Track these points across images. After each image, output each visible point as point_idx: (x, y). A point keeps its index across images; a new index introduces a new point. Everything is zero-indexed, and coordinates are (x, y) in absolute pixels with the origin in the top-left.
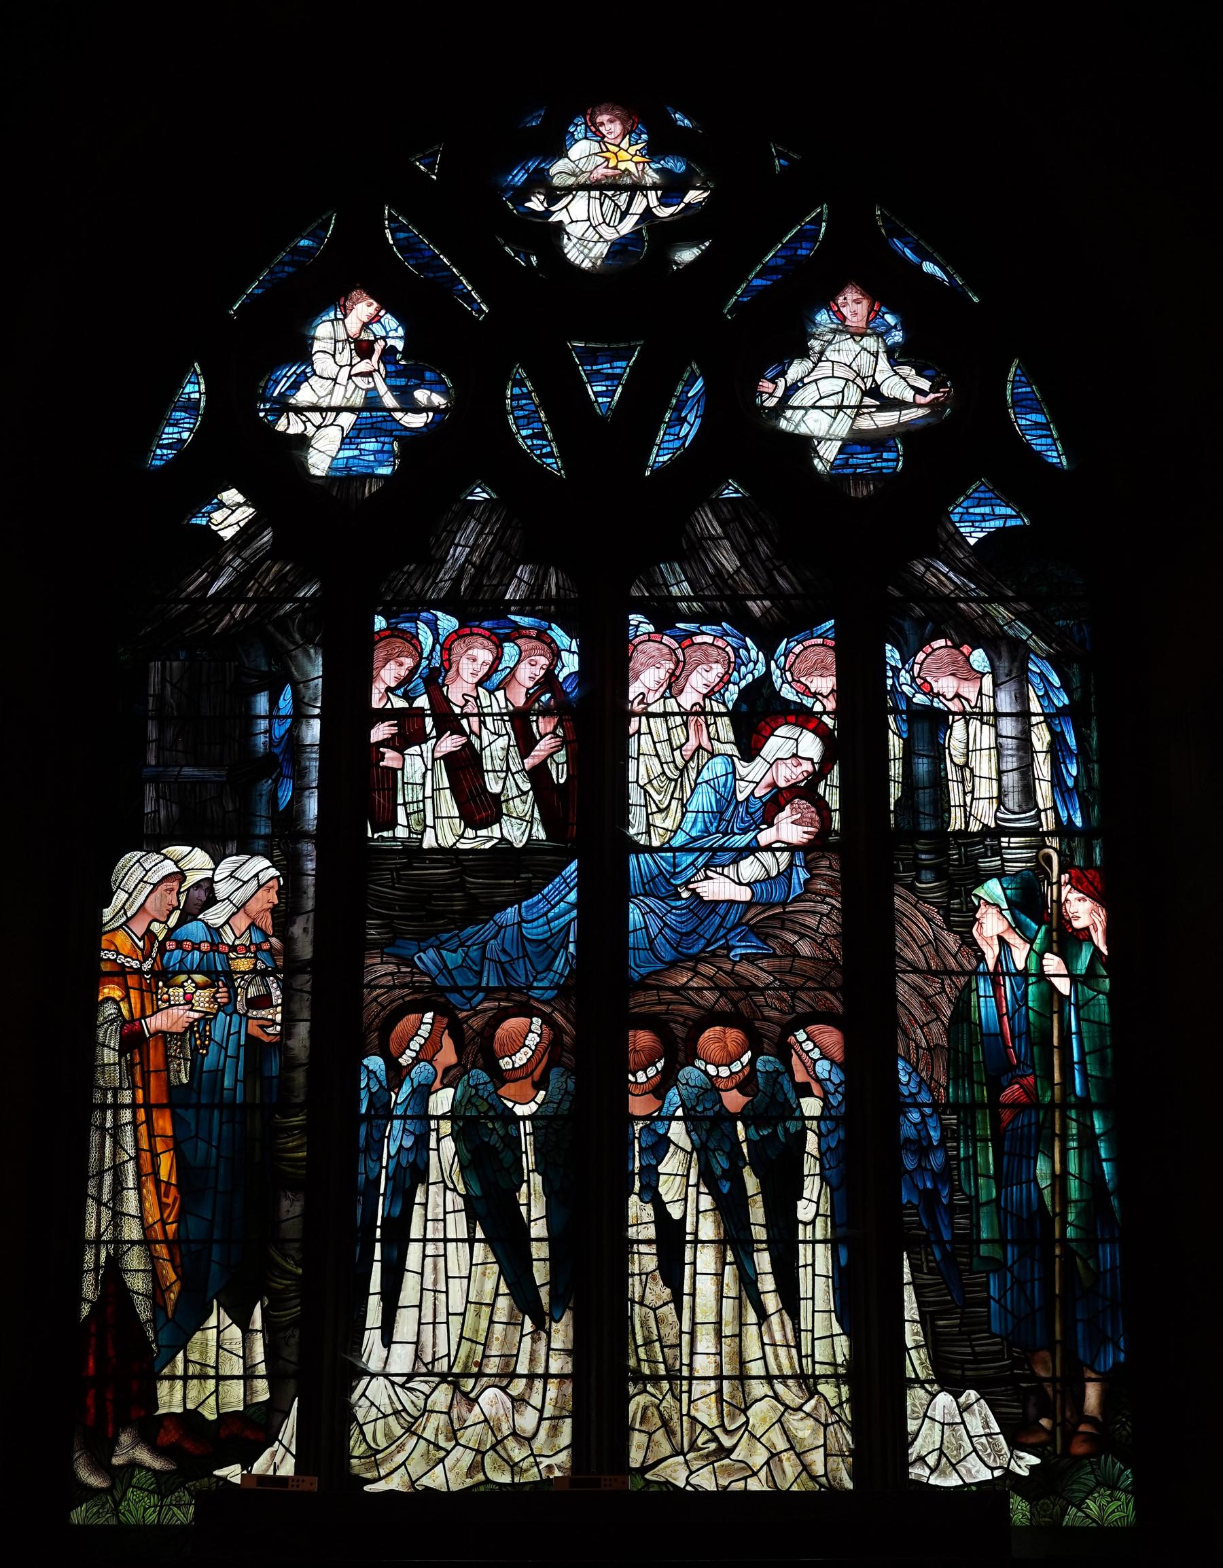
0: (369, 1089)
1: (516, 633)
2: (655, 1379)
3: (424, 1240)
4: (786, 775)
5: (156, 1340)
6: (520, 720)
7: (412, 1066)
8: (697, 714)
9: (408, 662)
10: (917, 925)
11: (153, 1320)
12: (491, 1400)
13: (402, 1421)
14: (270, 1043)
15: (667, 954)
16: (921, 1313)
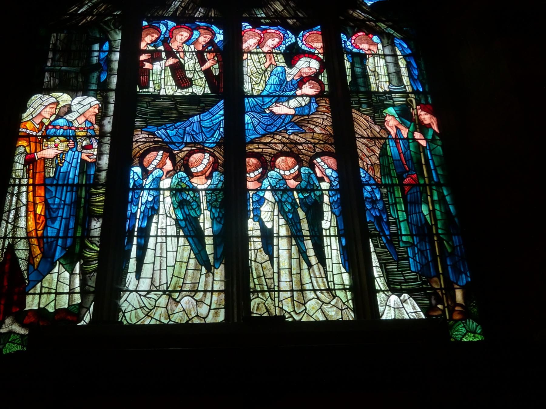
0: (134, 179)
1: (198, 28)
2: (263, 291)
3: (156, 236)
4: (306, 72)
5: (28, 278)
7: (153, 170)
8: (270, 53)
9: (156, 36)
10: (362, 124)
11: (28, 270)
12: (186, 301)
13: (144, 311)
14: (91, 162)
15: (262, 132)
16: (380, 264)
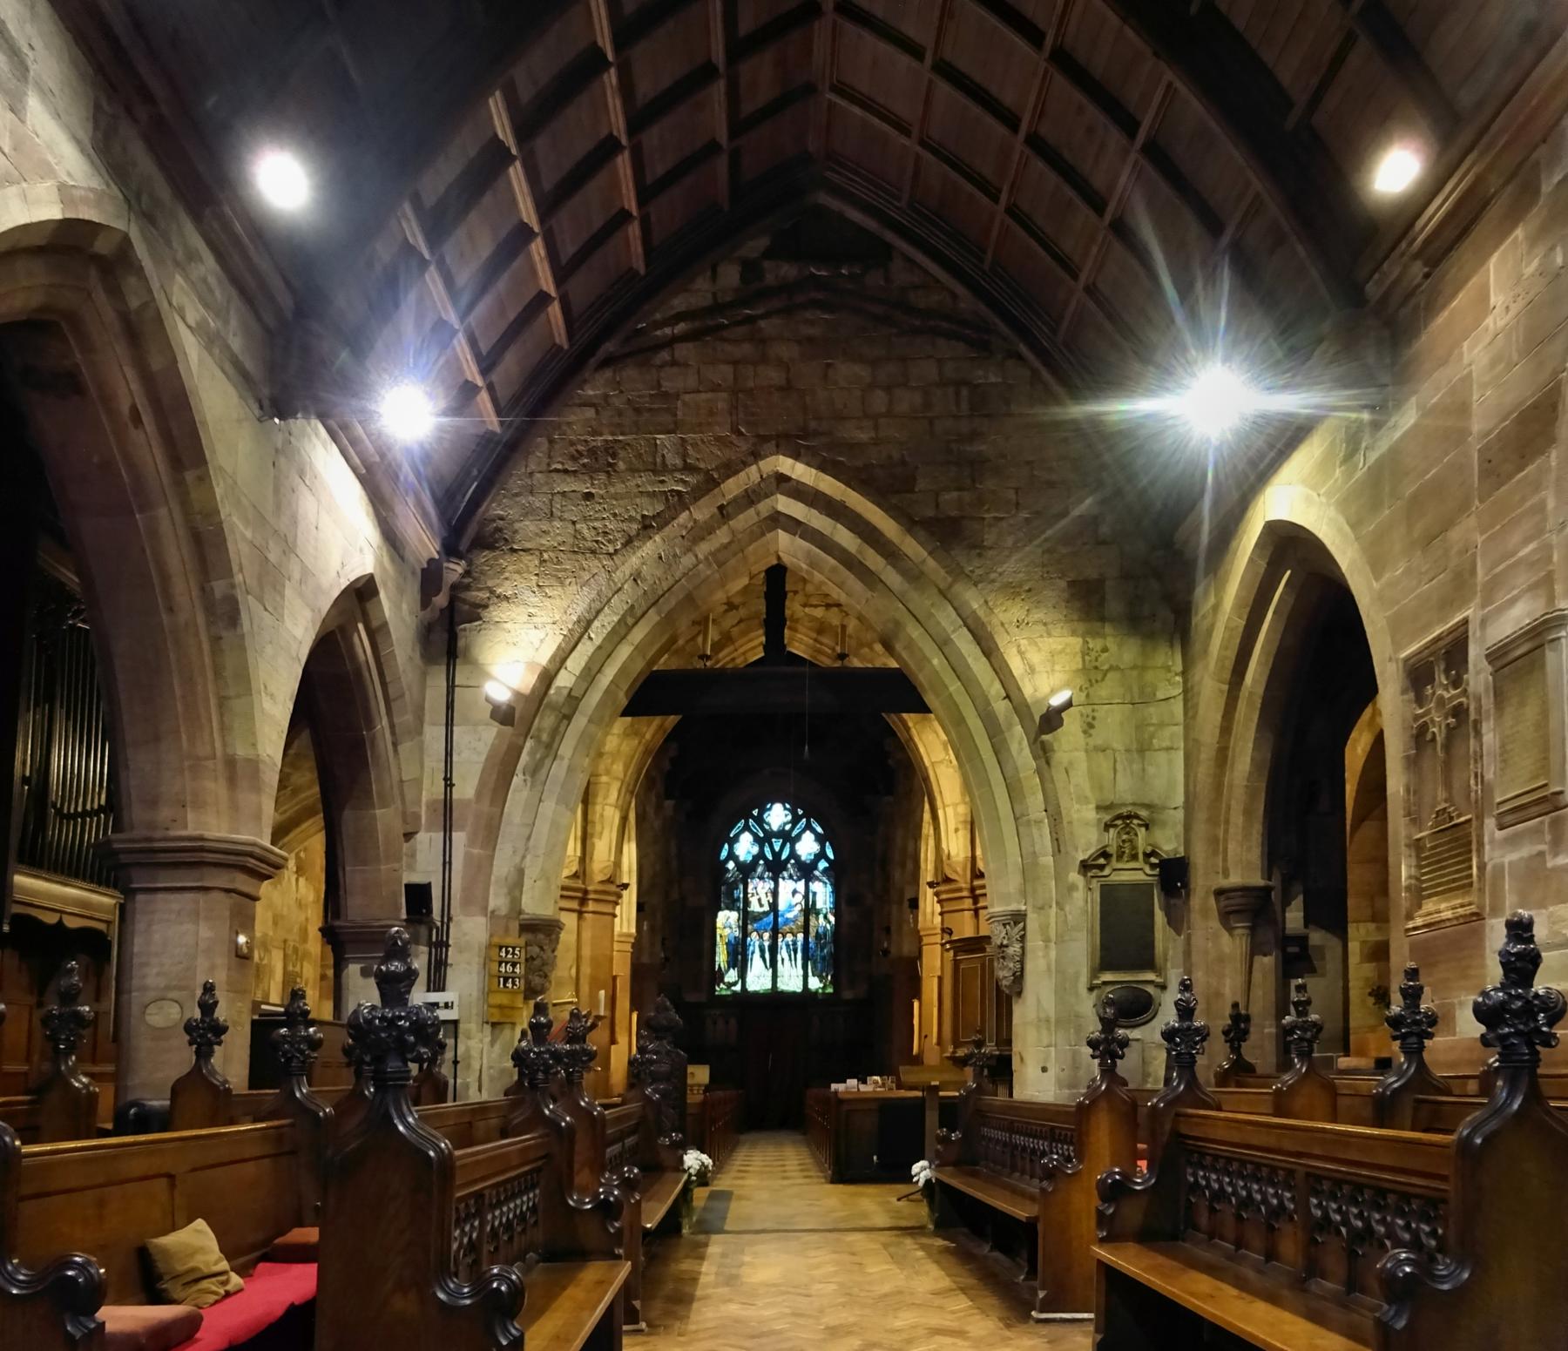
10: (813, 921)
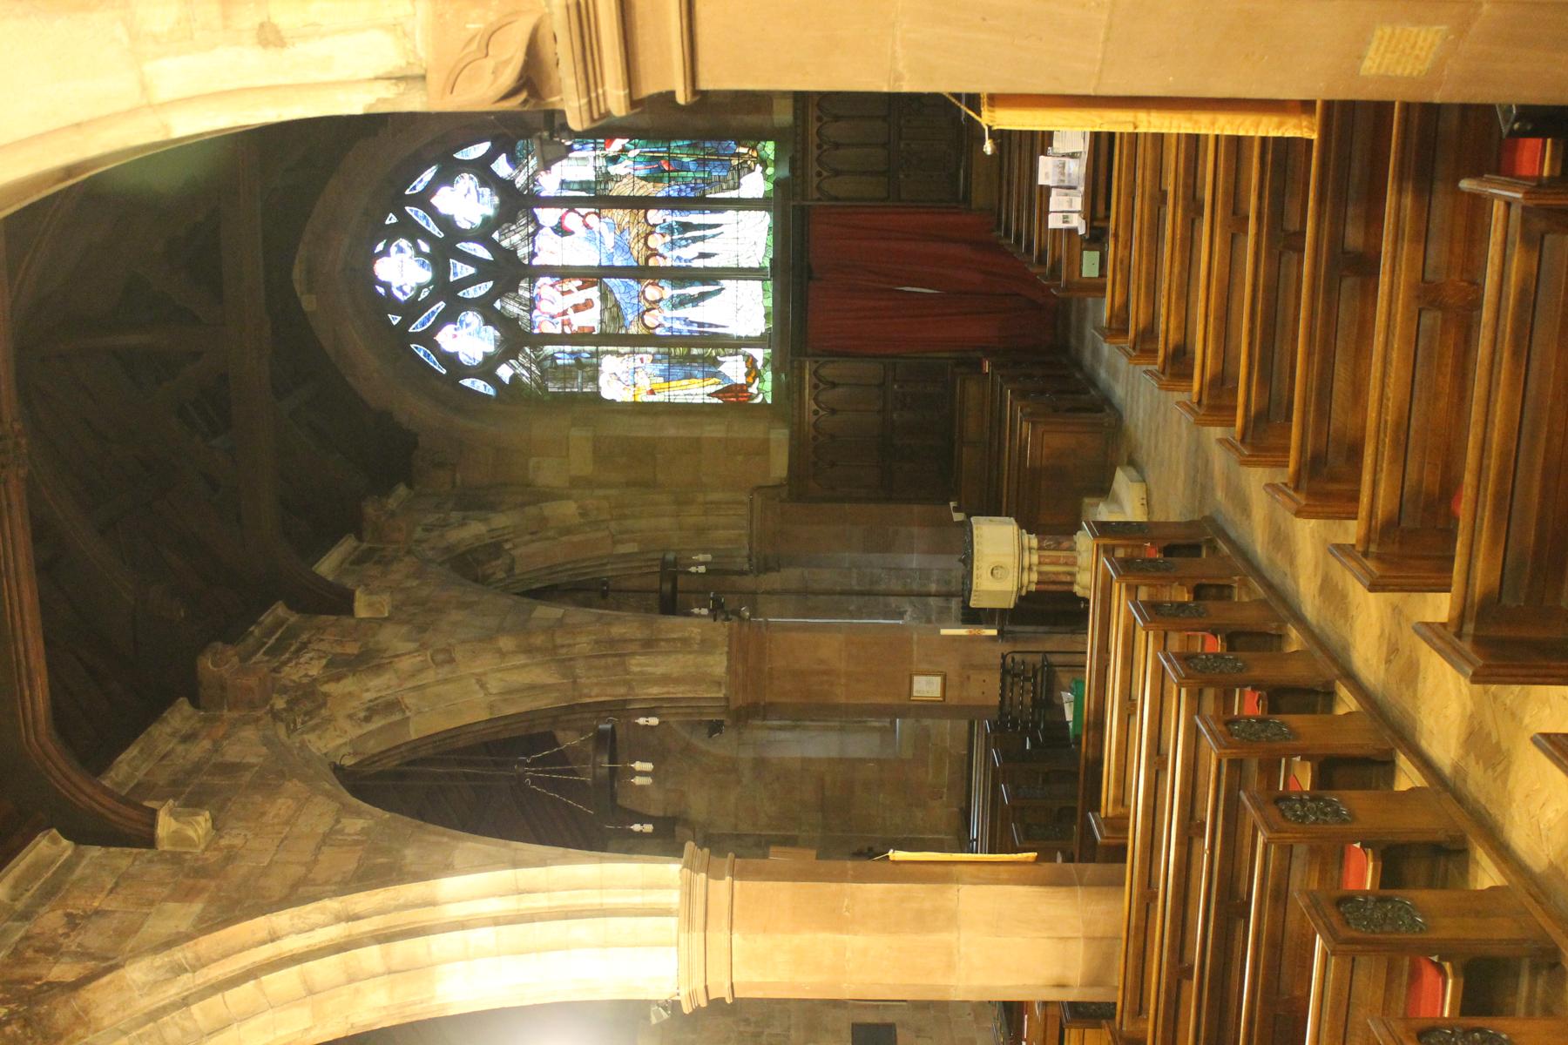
6: (563, 293)
10: (619, 189)
